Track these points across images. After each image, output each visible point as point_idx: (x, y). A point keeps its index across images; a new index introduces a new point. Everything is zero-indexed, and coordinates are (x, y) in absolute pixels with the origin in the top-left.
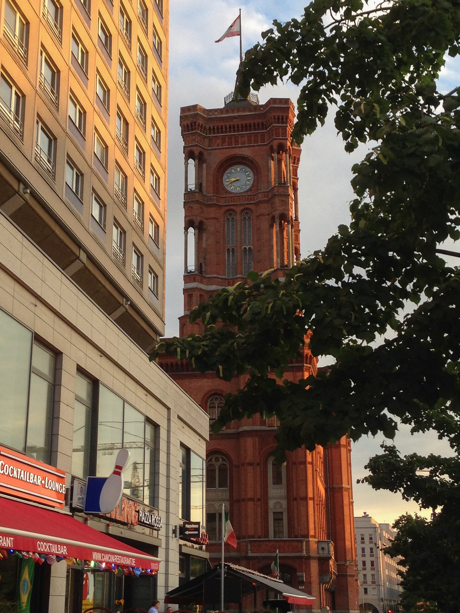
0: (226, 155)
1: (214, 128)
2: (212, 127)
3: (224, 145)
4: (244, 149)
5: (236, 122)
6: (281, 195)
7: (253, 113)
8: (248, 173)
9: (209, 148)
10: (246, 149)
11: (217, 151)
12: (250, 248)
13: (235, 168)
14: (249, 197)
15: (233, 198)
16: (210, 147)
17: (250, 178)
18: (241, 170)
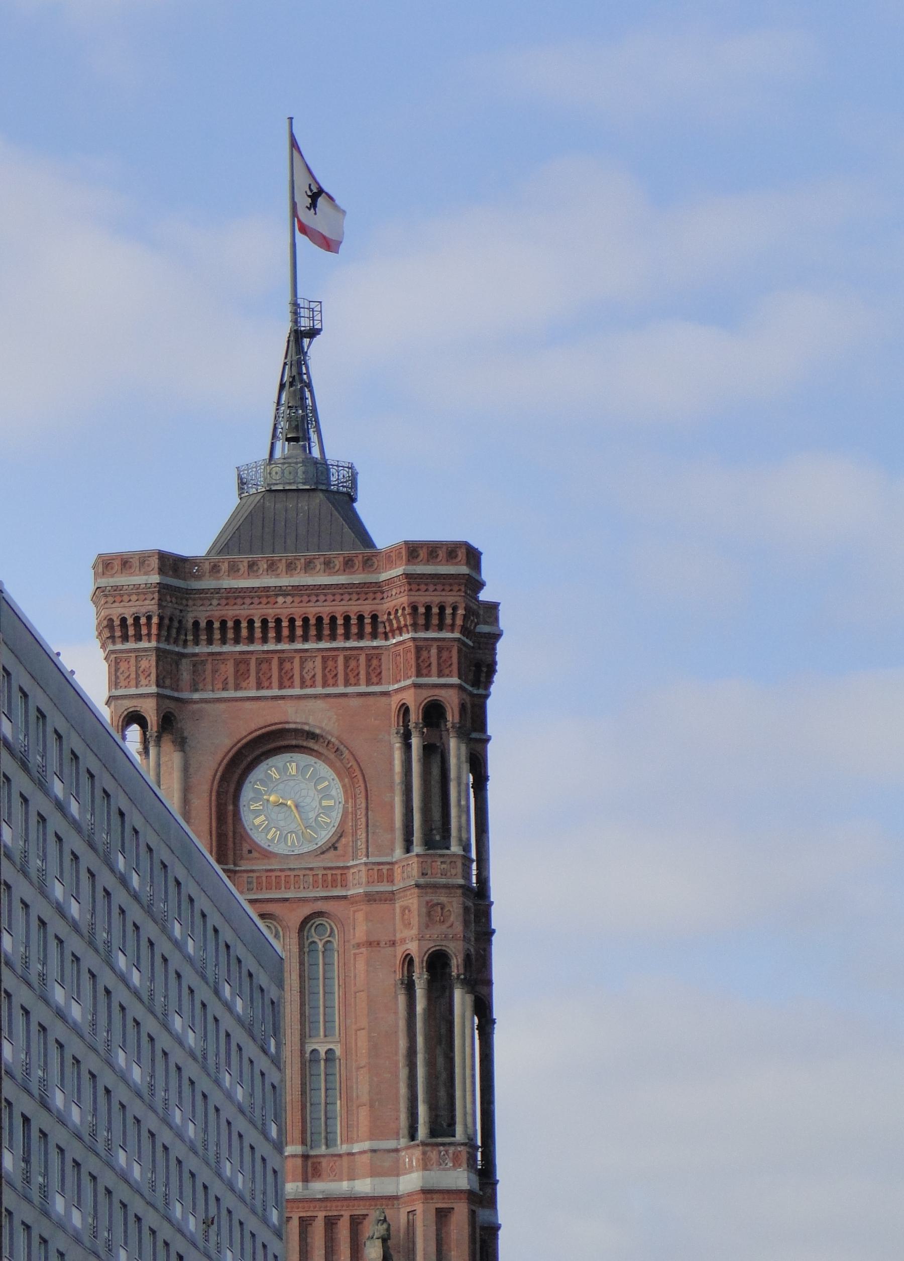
0: (253, 726)
1: (210, 623)
2: (203, 624)
3: (244, 684)
4: (311, 703)
5: (284, 608)
6: (435, 887)
7: (342, 579)
8: (326, 783)
9: (196, 696)
10: (320, 704)
11: (222, 706)
12: (330, 1051)
13: (280, 765)
14: (329, 872)
15: (274, 874)
16: (196, 690)
17: (332, 803)
18: (302, 771)
